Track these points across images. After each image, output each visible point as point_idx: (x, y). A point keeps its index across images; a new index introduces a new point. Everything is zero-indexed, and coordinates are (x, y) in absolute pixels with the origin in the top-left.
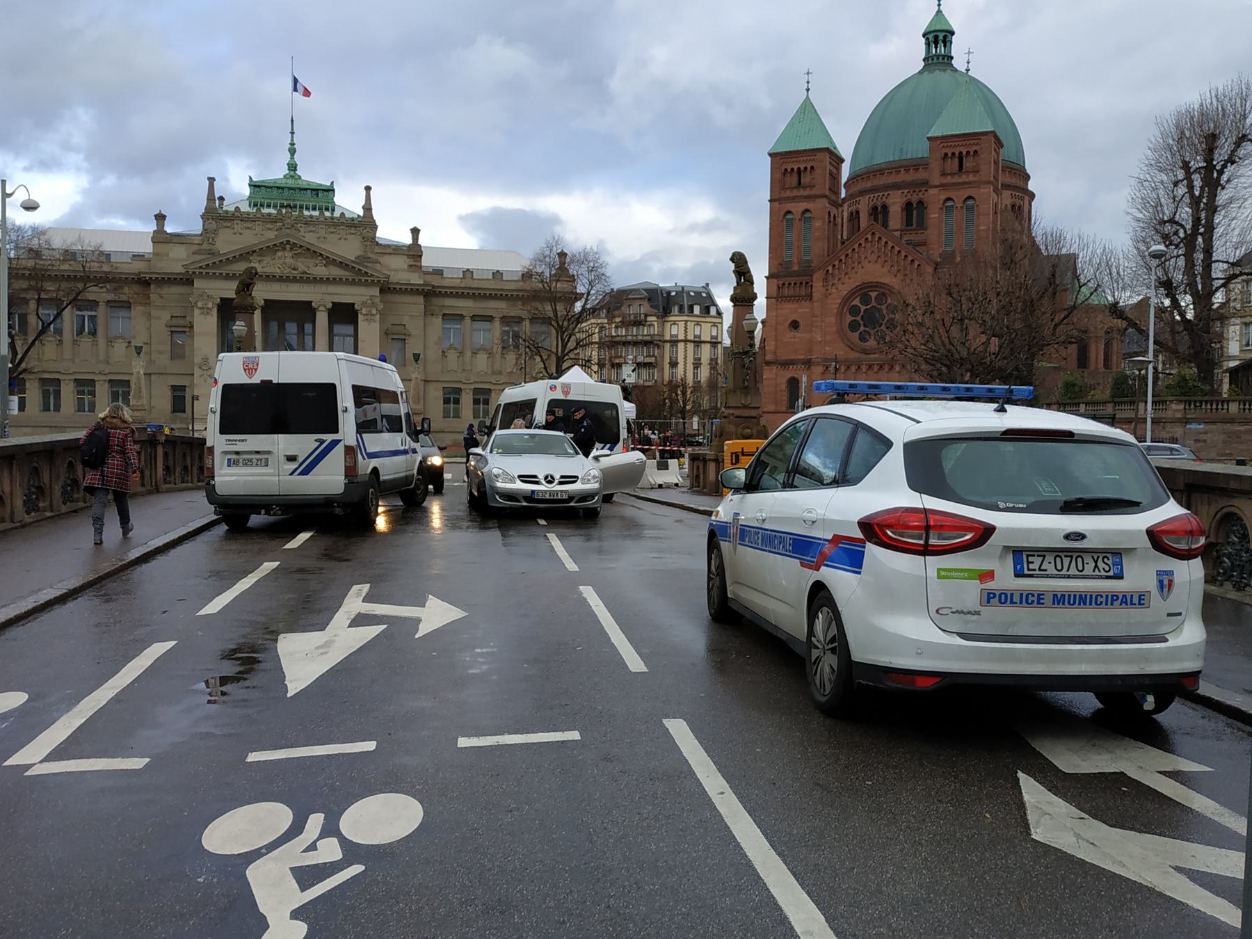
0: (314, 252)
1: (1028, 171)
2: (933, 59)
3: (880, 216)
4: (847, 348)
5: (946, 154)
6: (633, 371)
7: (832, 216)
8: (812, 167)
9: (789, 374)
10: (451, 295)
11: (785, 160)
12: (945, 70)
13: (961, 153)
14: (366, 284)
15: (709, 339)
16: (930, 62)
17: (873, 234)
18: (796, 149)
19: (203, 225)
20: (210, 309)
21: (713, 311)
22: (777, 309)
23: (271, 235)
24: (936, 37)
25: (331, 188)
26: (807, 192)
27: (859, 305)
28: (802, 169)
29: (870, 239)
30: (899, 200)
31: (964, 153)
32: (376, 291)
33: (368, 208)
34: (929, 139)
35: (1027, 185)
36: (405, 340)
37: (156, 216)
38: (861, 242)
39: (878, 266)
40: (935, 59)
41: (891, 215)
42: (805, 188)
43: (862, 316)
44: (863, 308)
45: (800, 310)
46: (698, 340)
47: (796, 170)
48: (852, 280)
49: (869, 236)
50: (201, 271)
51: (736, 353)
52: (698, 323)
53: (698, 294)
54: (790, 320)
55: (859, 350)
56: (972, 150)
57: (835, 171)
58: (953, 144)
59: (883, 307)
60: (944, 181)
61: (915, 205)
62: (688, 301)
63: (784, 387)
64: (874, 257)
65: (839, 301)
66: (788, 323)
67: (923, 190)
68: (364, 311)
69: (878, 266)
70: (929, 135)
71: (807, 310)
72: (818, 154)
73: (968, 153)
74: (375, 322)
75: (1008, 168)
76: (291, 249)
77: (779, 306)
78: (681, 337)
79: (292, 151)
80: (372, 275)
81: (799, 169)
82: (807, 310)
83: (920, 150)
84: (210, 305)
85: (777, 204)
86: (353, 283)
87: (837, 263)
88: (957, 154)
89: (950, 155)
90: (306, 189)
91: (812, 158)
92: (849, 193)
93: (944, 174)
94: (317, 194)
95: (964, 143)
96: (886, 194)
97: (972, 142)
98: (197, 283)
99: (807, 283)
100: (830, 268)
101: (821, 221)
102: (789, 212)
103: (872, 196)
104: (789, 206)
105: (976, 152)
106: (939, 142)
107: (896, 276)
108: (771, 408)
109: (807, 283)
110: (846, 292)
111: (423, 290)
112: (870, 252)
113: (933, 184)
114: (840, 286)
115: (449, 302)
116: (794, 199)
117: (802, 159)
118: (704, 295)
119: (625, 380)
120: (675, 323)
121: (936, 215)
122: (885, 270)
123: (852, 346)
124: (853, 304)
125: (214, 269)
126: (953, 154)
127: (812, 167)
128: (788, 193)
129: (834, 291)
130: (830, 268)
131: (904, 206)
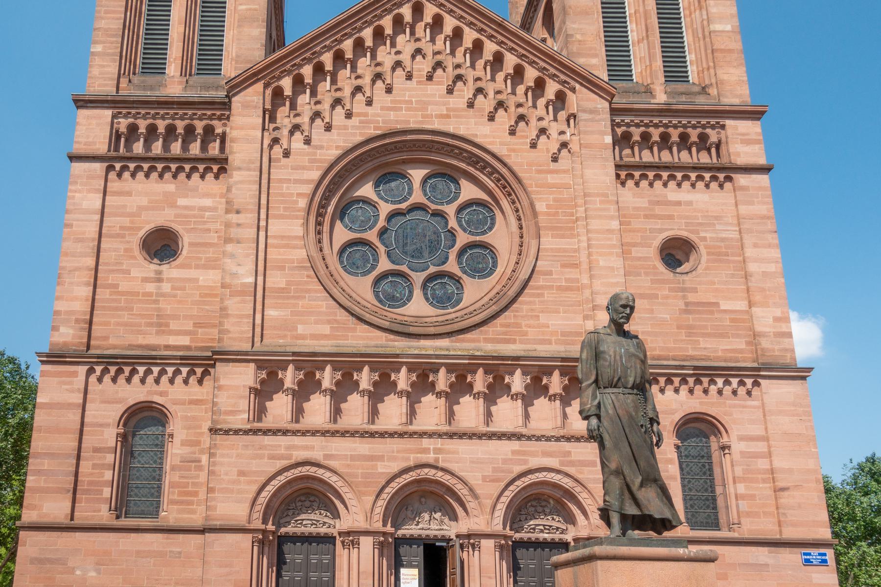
4: (342, 315)
39: (437, 89)
48: (355, 121)
55: (386, 324)
59: (450, 210)
63: (110, 436)
64: (423, 66)
65: (316, 175)
69: (437, 89)
77: (114, 184)
107: (491, 118)
114: (318, 132)
123: (357, 310)
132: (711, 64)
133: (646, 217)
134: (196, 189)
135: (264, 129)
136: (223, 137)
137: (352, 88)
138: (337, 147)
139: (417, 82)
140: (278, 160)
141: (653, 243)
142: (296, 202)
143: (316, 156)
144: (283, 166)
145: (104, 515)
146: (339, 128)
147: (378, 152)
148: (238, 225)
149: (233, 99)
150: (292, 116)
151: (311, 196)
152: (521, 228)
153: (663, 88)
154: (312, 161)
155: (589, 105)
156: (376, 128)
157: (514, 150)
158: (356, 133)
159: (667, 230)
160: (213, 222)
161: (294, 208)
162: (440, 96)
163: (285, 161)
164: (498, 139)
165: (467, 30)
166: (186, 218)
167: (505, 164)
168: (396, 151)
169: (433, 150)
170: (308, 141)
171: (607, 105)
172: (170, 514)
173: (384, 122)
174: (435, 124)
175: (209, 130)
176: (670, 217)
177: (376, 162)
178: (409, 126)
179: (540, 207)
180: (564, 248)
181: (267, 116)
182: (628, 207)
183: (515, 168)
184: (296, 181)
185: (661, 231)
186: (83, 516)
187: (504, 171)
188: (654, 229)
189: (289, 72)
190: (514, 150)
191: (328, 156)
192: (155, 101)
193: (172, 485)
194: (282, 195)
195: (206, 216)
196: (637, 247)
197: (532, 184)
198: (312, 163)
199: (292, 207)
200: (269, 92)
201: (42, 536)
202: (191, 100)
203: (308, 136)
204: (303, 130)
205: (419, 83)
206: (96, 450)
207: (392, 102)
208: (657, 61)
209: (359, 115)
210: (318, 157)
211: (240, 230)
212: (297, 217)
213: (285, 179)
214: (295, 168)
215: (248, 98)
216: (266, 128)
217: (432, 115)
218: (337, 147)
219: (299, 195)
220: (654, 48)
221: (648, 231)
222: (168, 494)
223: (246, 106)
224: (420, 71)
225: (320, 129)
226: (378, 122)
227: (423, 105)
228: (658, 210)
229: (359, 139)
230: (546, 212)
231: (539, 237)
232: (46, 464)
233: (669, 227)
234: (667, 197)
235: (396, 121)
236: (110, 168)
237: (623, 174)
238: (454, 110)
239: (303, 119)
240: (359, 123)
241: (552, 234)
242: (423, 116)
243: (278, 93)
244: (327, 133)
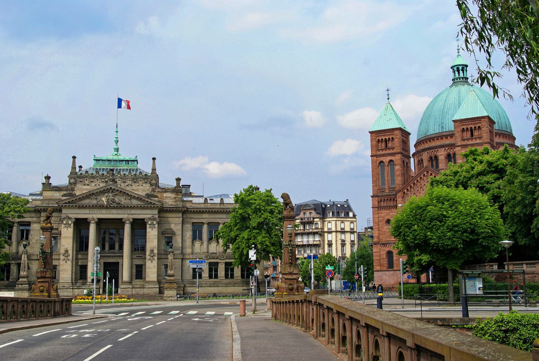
0: (124, 193)
1: (514, 135)
2: (457, 80)
3: (434, 162)
5: (463, 129)
6: (254, 254)
7: (405, 163)
8: (393, 138)
9: (387, 249)
10: (194, 212)
11: (378, 135)
12: (464, 85)
13: (471, 128)
14: (151, 208)
15: (349, 230)
16: (456, 81)
17: (428, 172)
18: (383, 129)
19: (69, 181)
20: (70, 225)
21: (351, 215)
22: (378, 213)
23: (102, 185)
24: (458, 69)
25: (135, 159)
26: (391, 151)
28: (387, 139)
29: (426, 175)
30: (444, 153)
31: (473, 128)
32: (156, 212)
33: (154, 170)
34: (454, 121)
35: (514, 142)
36: (172, 237)
37: (45, 177)
38: (421, 176)
40: (458, 79)
41: (440, 162)
42: (389, 149)
45: (391, 214)
46: (343, 230)
47: (384, 140)
48: (418, 197)
49: (425, 173)
50: (65, 205)
51: (285, 245)
52: (342, 222)
53: (342, 206)
54: (386, 219)
56: (477, 126)
57: (406, 139)
58: (467, 123)
60: (464, 143)
61: (452, 156)
62: (336, 210)
63: (385, 256)
66: (385, 220)
67: (453, 148)
68: (149, 222)
70: (454, 119)
72: (395, 131)
73: (475, 128)
74: (155, 228)
75: (502, 134)
76: (112, 192)
77: (380, 212)
78: (334, 229)
79: (117, 142)
80: (154, 204)
81: (386, 139)
83: (450, 127)
84: (70, 222)
85: (375, 158)
86: (144, 208)
87: (409, 188)
88: (469, 129)
89: (465, 129)
90: (122, 161)
91: (392, 133)
92: (417, 150)
93: (464, 140)
94: (128, 163)
95: (473, 123)
96: (436, 150)
97: (477, 122)
98: (64, 211)
99: (394, 199)
100: (405, 191)
101: (399, 166)
102: (382, 162)
103: (429, 152)
104: (382, 159)
105: (479, 127)
106: (459, 123)
108: (378, 268)
109: (394, 199)
111: (182, 210)
112: (426, 181)
113: (457, 145)
115: (192, 216)
116: (384, 155)
117: (387, 134)
118: (346, 206)
119: (250, 258)
120: (329, 222)
125: (72, 204)
126: (467, 128)
127: (393, 138)
128: (381, 152)
130: (405, 191)
131: (446, 156)
134: (393, 211)
145: (385, 269)
172: (395, 268)
186: (382, 269)
193: (395, 264)
200: (403, 193)
201: (377, 273)
206: (383, 259)
222: (395, 265)
232: (376, 261)
236: (379, 209)
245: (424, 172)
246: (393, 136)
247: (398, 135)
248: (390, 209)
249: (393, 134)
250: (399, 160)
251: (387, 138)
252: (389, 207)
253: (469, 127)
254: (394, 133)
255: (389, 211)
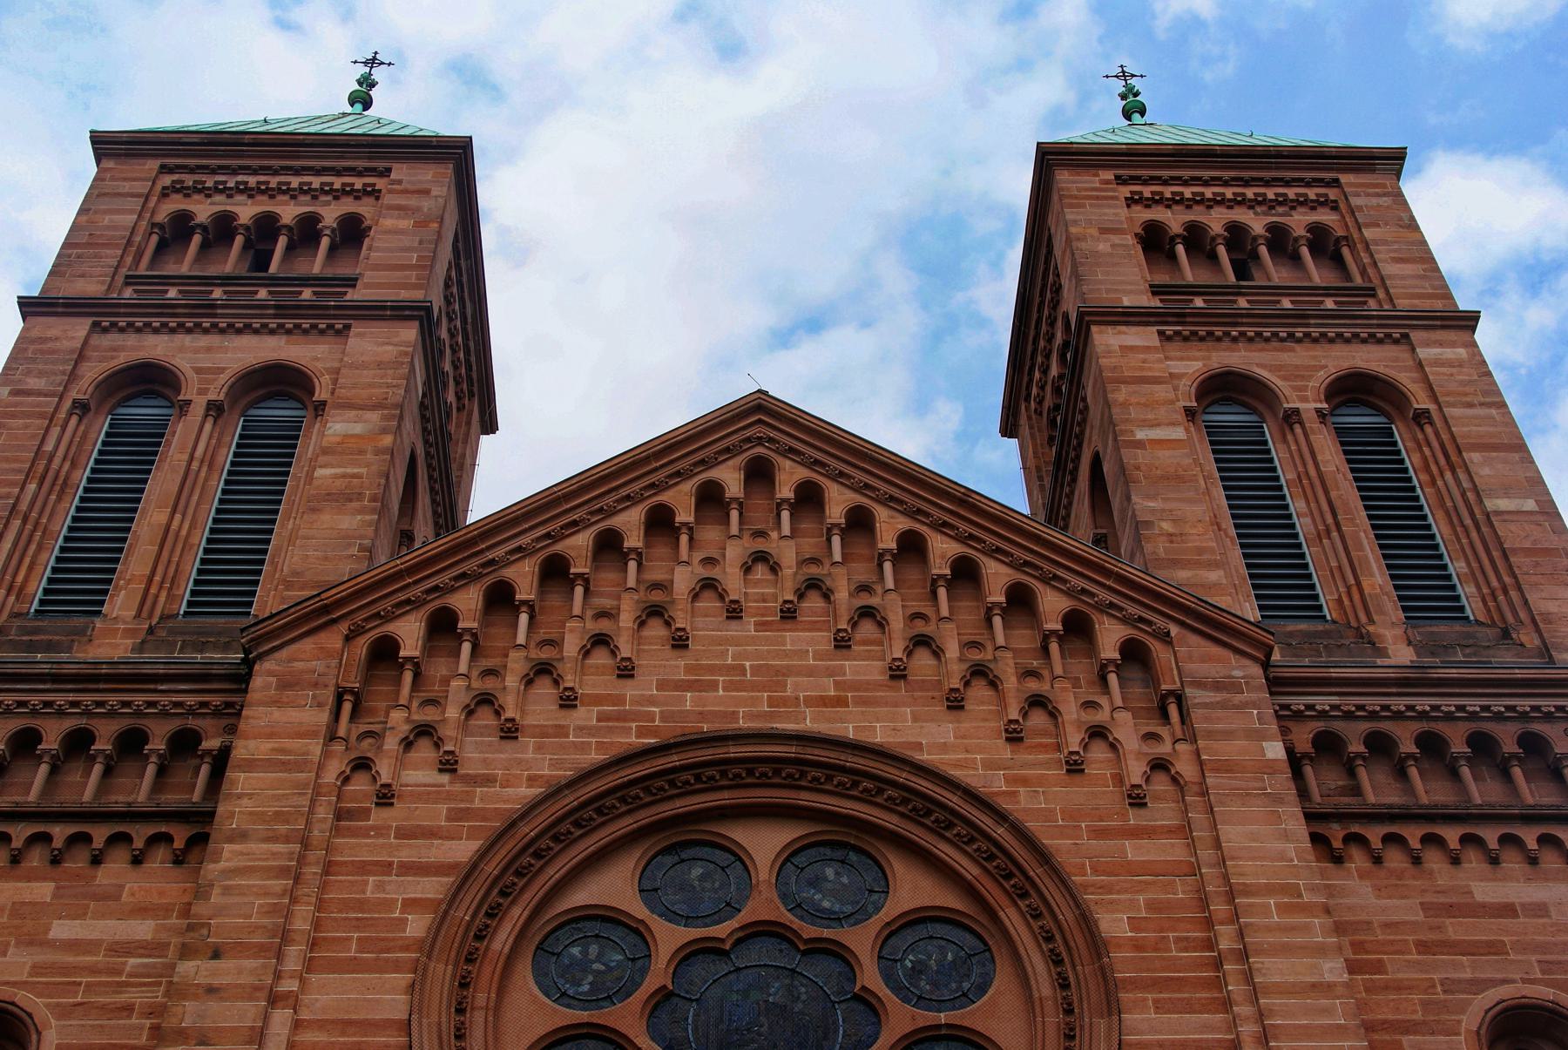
27: (638, 909)
38: (665, 497)
43: (663, 997)
44: (669, 938)
45: (61, 930)
48: (584, 715)
49: (731, 478)
65: (463, 850)
71: (143, 929)
82: (143, 929)
101: (374, 417)
104: (157, 348)
106: (1109, 175)
107: (955, 704)
110: (528, 792)
121: (1178, 433)
122: (863, 667)
124: (583, 896)
129: (420, 773)
130: (410, 633)
132: (1507, 580)
133: (1424, 947)
135: (332, 737)
136: (221, 761)
137: (582, 639)
138: (532, 780)
139: (756, 624)
140: (365, 813)
141: (1459, 1022)
142: (403, 922)
143: (472, 801)
144: (372, 828)
146: (542, 732)
147: (647, 790)
148: (211, 990)
149: (257, 667)
150: (415, 704)
151: (444, 906)
152: (1065, 985)
153: (1399, 631)
154: (456, 815)
155: (1213, 671)
156: (641, 732)
157: (1025, 781)
158: (589, 743)
159: (1494, 983)
160: (144, 984)
161: (394, 939)
162: (818, 656)
163: (378, 816)
164: (980, 753)
165: (881, 513)
166: (65, 975)
167: (1001, 816)
168: (697, 786)
169: (803, 783)
170: (448, 765)
171: (1256, 670)
173: (665, 717)
174: (805, 719)
175: (184, 743)
176: (1494, 948)
177: (645, 817)
178: (735, 726)
179: (1114, 924)
180: (1194, 1041)
181: (347, 707)
182: (1369, 923)
183: (1032, 825)
184: (408, 869)
185: (1478, 986)
187: (1000, 833)
188: (1453, 981)
189: (412, 604)
190: (1025, 781)
191: (505, 802)
192: (48, 674)
194: (361, 905)
195: (128, 969)
196: (1415, 1033)
197: (1084, 865)
198: (460, 820)
199: (383, 939)
200: (362, 646)
202: (147, 670)
203: (452, 753)
204: (439, 738)
205: (761, 626)
207: (689, 669)
208: (1372, 575)
209: (597, 700)
210: (477, 804)
211: (213, 1006)
212: (397, 967)
213: (377, 863)
214: (405, 834)
215: (299, 665)
216: (342, 732)
217: (797, 698)
218: (532, 780)
219: (410, 904)
220: (1360, 548)
221: (1439, 988)
223: (287, 683)
224: (764, 601)
225: (489, 736)
226: (650, 717)
227: (773, 678)
228: (1454, 929)
229: (595, 757)
230: (1131, 938)
231: (1112, 1007)
233: (1499, 976)
234: (1471, 893)
235: (701, 713)
237: (1336, 833)
238: (855, 686)
239: (444, 712)
240: (599, 720)
241: (1156, 1001)
242: (771, 704)
243: (385, 653)
244: (509, 745)
245: (706, 464)
246: (365, 208)
247: (427, 192)
248: (77, 862)
249: (375, 194)
250: (380, 365)
251: (289, 212)
252: (60, 832)
253: (1216, 221)
254: (380, 183)
255: (43, 890)
